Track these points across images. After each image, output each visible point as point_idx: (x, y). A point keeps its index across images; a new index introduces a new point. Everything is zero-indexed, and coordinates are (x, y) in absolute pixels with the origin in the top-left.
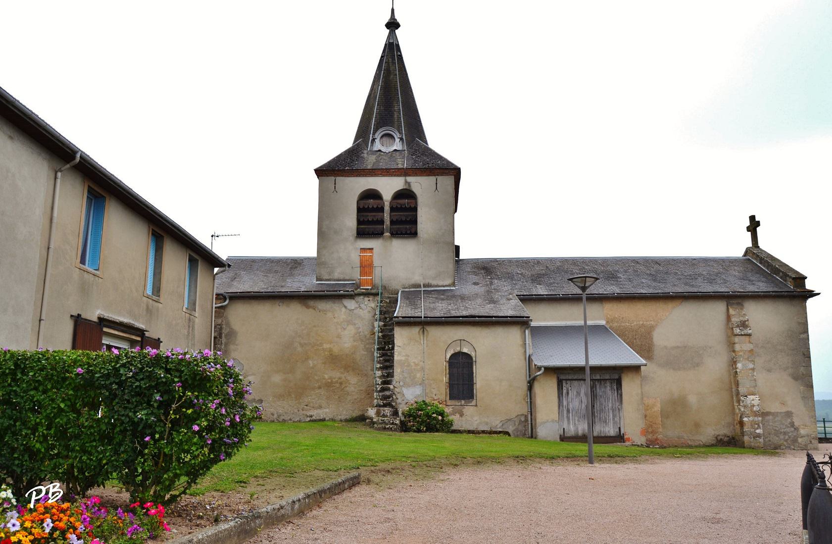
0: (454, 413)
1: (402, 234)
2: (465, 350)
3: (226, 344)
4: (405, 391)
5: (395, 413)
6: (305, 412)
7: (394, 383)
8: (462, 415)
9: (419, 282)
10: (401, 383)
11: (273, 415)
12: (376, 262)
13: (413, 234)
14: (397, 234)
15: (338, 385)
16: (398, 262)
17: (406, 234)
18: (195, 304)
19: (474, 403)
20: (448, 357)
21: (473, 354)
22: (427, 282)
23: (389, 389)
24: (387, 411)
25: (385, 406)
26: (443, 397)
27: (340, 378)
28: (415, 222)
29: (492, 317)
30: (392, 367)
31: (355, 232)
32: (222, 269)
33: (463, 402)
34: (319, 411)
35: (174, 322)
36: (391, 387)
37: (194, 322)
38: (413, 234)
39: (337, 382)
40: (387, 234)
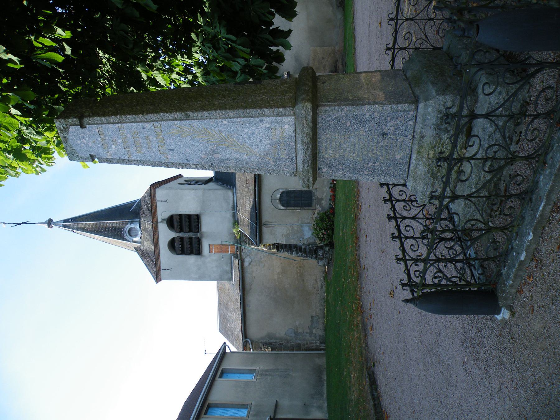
0: (321, 205)
1: (198, 225)
2: (278, 196)
3: (276, 339)
4: (306, 237)
5: (321, 248)
6: (319, 288)
7: (301, 244)
8: (322, 199)
9: (231, 214)
10: (301, 239)
11: (321, 309)
12: (218, 242)
13: (198, 217)
14: (198, 228)
15: (302, 269)
16: (216, 228)
17: (198, 222)
18: (251, 370)
19: (314, 191)
20: (283, 208)
21: (281, 191)
22: (230, 208)
23: (305, 249)
24: (320, 253)
25: (316, 253)
26: (310, 212)
27: (297, 268)
28: (189, 216)
29: (255, 190)
30: (290, 245)
31: (198, 257)
32: (227, 347)
33: (314, 198)
34: (318, 280)
35: (264, 389)
36: (303, 247)
37: (263, 370)
38: (198, 217)
39: (300, 270)
40: (199, 235)
